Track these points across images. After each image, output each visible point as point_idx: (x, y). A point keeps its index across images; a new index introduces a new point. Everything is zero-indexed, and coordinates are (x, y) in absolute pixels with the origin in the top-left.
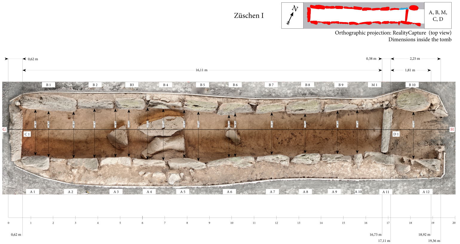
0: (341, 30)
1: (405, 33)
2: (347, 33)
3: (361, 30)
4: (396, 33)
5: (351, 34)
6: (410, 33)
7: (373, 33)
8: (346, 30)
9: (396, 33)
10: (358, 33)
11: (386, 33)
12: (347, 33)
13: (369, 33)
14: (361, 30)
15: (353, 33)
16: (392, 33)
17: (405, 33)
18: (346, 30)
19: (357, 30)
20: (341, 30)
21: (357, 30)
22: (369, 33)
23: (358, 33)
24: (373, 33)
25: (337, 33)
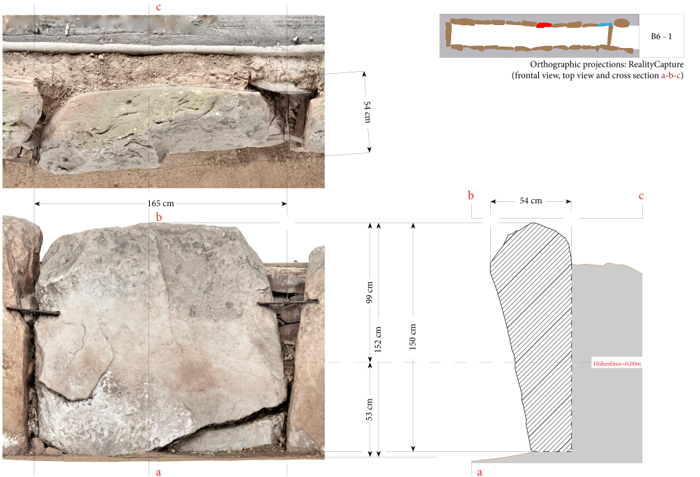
0: (539, 60)
1: (650, 65)
2: (551, 65)
3: (573, 60)
4: (633, 65)
5: (557, 66)
6: (657, 64)
8: (548, 60)
9: (633, 65)
10: (567, 65)
12: (551, 65)
14: (573, 60)
16: (628, 65)
17: (650, 65)
18: (548, 60)
19: (566, 60)
20: (539, 60)
21: (566, 60)
23: (567, 65)
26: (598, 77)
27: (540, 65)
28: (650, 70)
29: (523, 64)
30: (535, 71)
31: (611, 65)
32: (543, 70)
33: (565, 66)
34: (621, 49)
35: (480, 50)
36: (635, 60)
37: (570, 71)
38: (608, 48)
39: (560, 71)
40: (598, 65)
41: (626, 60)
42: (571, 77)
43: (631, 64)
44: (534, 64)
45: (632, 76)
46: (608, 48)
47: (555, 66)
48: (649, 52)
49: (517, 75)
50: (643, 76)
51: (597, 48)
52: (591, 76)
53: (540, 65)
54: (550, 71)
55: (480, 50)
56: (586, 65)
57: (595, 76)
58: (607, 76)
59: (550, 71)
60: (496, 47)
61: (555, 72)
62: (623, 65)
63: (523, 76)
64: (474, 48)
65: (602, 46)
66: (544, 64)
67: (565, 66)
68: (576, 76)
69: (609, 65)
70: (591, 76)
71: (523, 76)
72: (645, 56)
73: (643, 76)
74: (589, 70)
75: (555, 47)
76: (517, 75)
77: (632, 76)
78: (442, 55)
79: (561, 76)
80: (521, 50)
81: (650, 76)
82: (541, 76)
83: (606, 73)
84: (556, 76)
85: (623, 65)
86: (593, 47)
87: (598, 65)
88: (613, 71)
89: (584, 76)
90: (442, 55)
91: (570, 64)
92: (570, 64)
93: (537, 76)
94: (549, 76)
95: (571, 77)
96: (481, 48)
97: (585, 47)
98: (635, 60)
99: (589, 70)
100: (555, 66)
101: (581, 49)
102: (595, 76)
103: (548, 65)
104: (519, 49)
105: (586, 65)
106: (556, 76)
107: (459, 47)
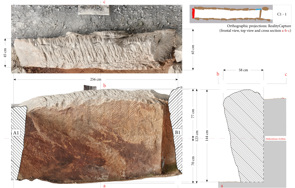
0: (231, 24)
1: (277, 26)
7: (253, 26)
8: (235, 24)
11: (262, 26)
13: (250, 26)
15: (240, 26)
17: (277, 26)
18: (235, 24)
19: (242, 24)
20: (231, 24)
21: (242, 24)
22: (250, 26)
24: (253, 26)
25: (229, 26)
26: (256, 31)
27: (231, 26)
28: (277, 29)
29: (224, 26)
30: (229, 29)
31: (261, 26)
32: (233, 29)
33: (242, 26)
34: (265, 19)
35: (207, 20)
36: (271, 24)
37: (244, 29)
38: (260, 19)
39: (240, 29)
40: (255, 26)
41: (267, 24)
42: (244, 31)
43: (269, 26)
44: (229, 26)
45: (270, 31)
46: (260, 19)
47: (238, 27)
48: (277, 21)
49: (222, 31)
50: (274, 31)
51: (255, 19)
52: (253, 31)
53: (231, 26)
54: (236, 29)
55: (207, 20)
56: (250, 26)
57: (254, 31)
58: (259, 31)
59: (236, 29)
60: (213, 19)
61: (238, 29)
62: (266, 26)
63: (224, 31)
64: (204, 19)
65: (257, 18)
66: (233, 26)
67: (242, 26)
68: (246, 31)
69: (260, 26)
70: (253, 31)
71: (224, 31)
72: (275, 22)
73: (274, 31)
74: (252, 29)
75: (237, 19)
76: (222, 31)
77: (270, 31)
78: (191, 22)
79: (240, 31)
80: (223, 20)
81: (277, 31)
82: (232, 31)
83: (259, 30)
84: (238, 31)
85: (266, 26)
86: (253, 19)
87: (255, 26)
88: (262, 29)
89: (250, 31)
90: (191, 22)
91: (244, 26)
92: (244, 26)
93: (230, 31)
94: (235, 31)
95: (244, 31)
96: (207, 19)
97: (250, 19)
98: (271, 24)
99: (252, 29)
100: (238, 27)
101: (249, 20)
102: (254, 31)
103: (235, 26)
104: (223, 19)
105: (250, 26)
106: (238, 31)
107: (198, 19)
